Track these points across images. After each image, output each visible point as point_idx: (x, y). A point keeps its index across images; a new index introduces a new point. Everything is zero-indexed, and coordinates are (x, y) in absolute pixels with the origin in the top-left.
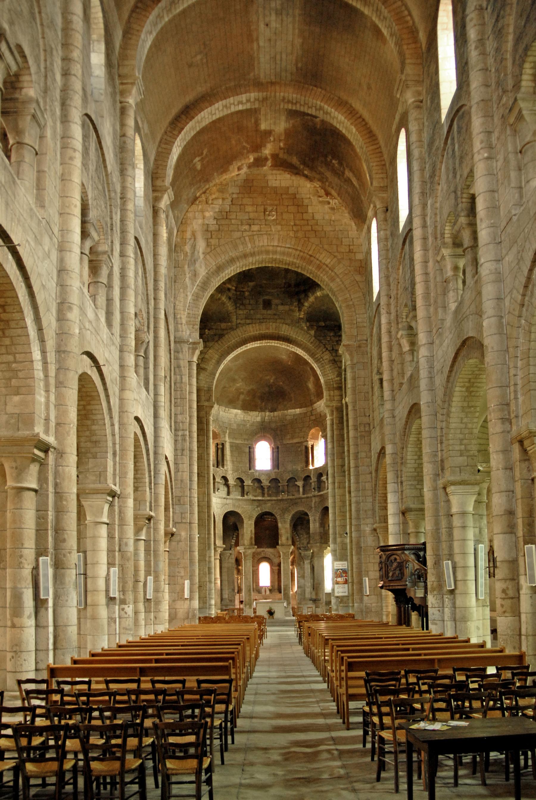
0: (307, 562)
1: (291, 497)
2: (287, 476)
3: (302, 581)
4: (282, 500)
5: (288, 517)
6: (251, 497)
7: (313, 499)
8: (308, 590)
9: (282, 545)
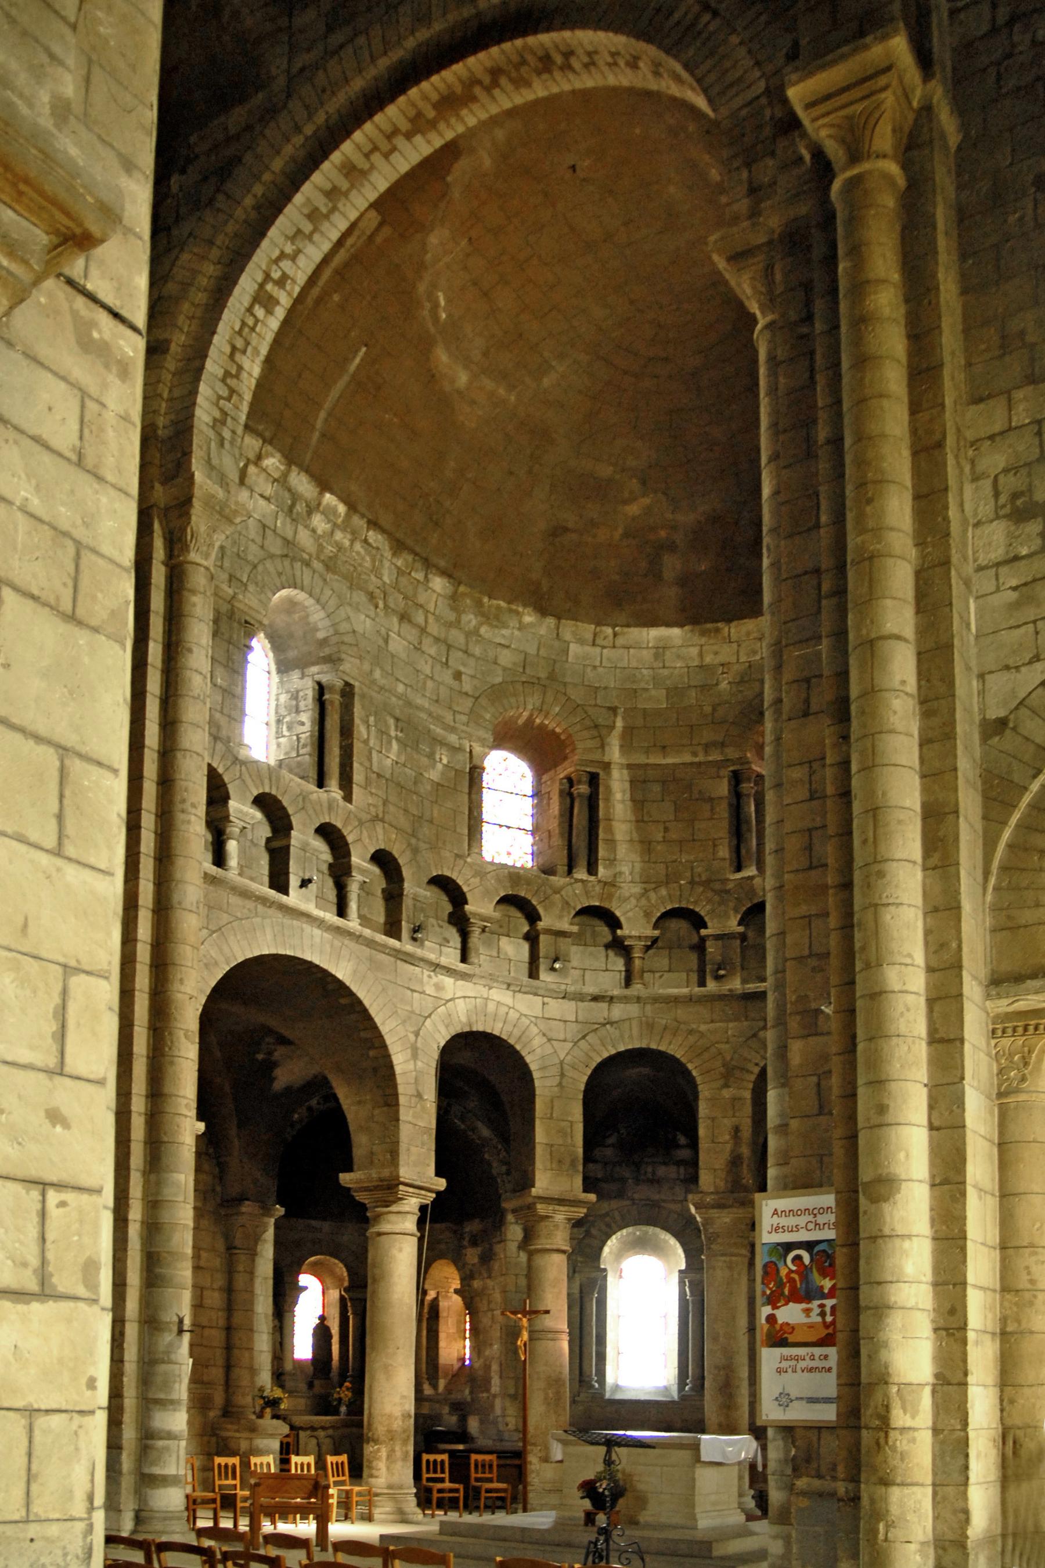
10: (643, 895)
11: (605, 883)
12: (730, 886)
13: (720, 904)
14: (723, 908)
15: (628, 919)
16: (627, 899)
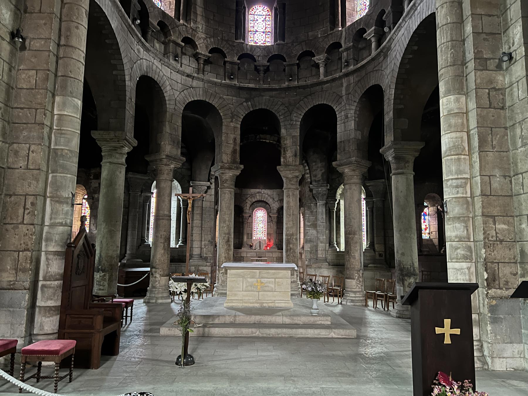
0: (320, 203)
1: (304, 83)
2: (298, 50)
3: (312, 232)
4: (288, 89)
5: (298, 118)
6: (235, 82)
7: (345, 81)
8: (322, 246)
9: (287, 165)
10: (205, 39)
11: (193, 30)
12: (235, 44)
13: (231, 50)
14: (232, 52)
15: (200, 47)
16: (200, 39)
